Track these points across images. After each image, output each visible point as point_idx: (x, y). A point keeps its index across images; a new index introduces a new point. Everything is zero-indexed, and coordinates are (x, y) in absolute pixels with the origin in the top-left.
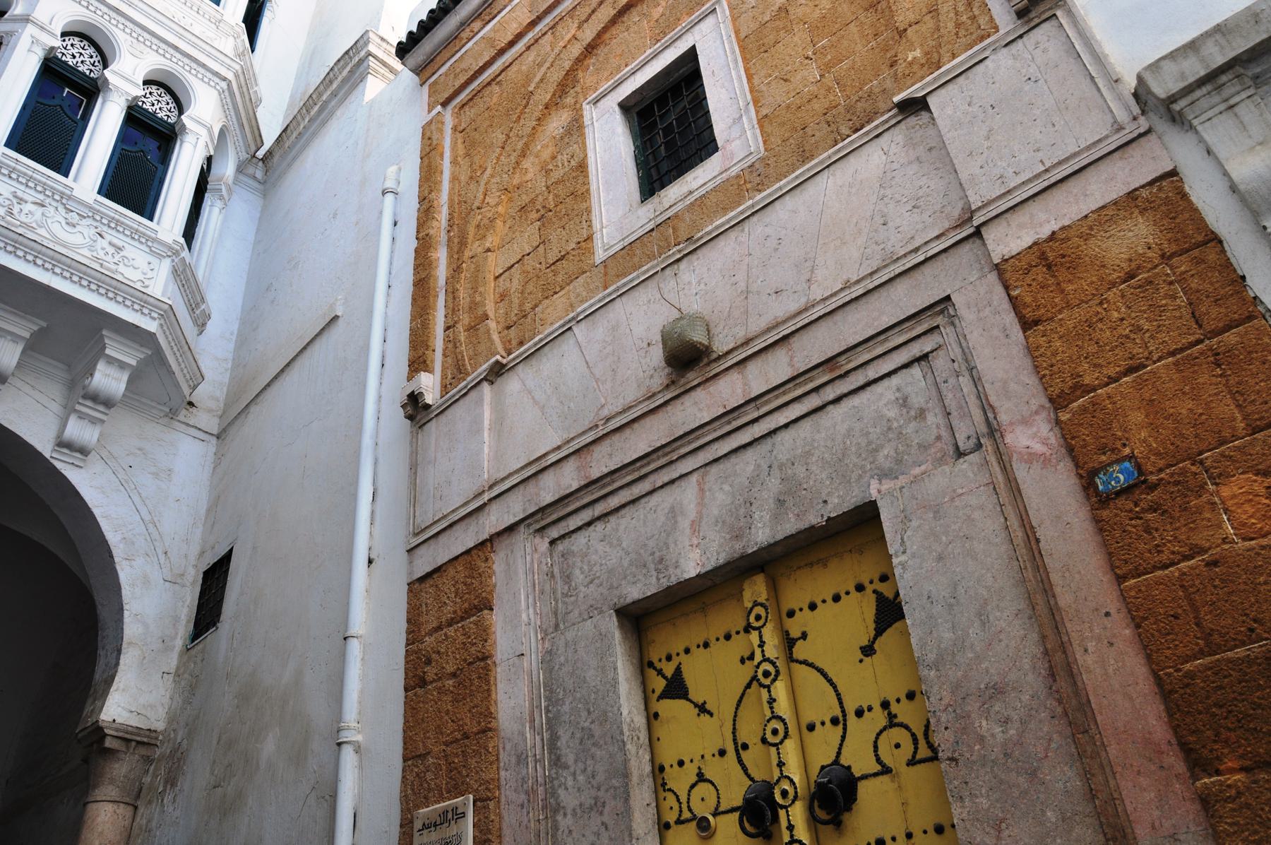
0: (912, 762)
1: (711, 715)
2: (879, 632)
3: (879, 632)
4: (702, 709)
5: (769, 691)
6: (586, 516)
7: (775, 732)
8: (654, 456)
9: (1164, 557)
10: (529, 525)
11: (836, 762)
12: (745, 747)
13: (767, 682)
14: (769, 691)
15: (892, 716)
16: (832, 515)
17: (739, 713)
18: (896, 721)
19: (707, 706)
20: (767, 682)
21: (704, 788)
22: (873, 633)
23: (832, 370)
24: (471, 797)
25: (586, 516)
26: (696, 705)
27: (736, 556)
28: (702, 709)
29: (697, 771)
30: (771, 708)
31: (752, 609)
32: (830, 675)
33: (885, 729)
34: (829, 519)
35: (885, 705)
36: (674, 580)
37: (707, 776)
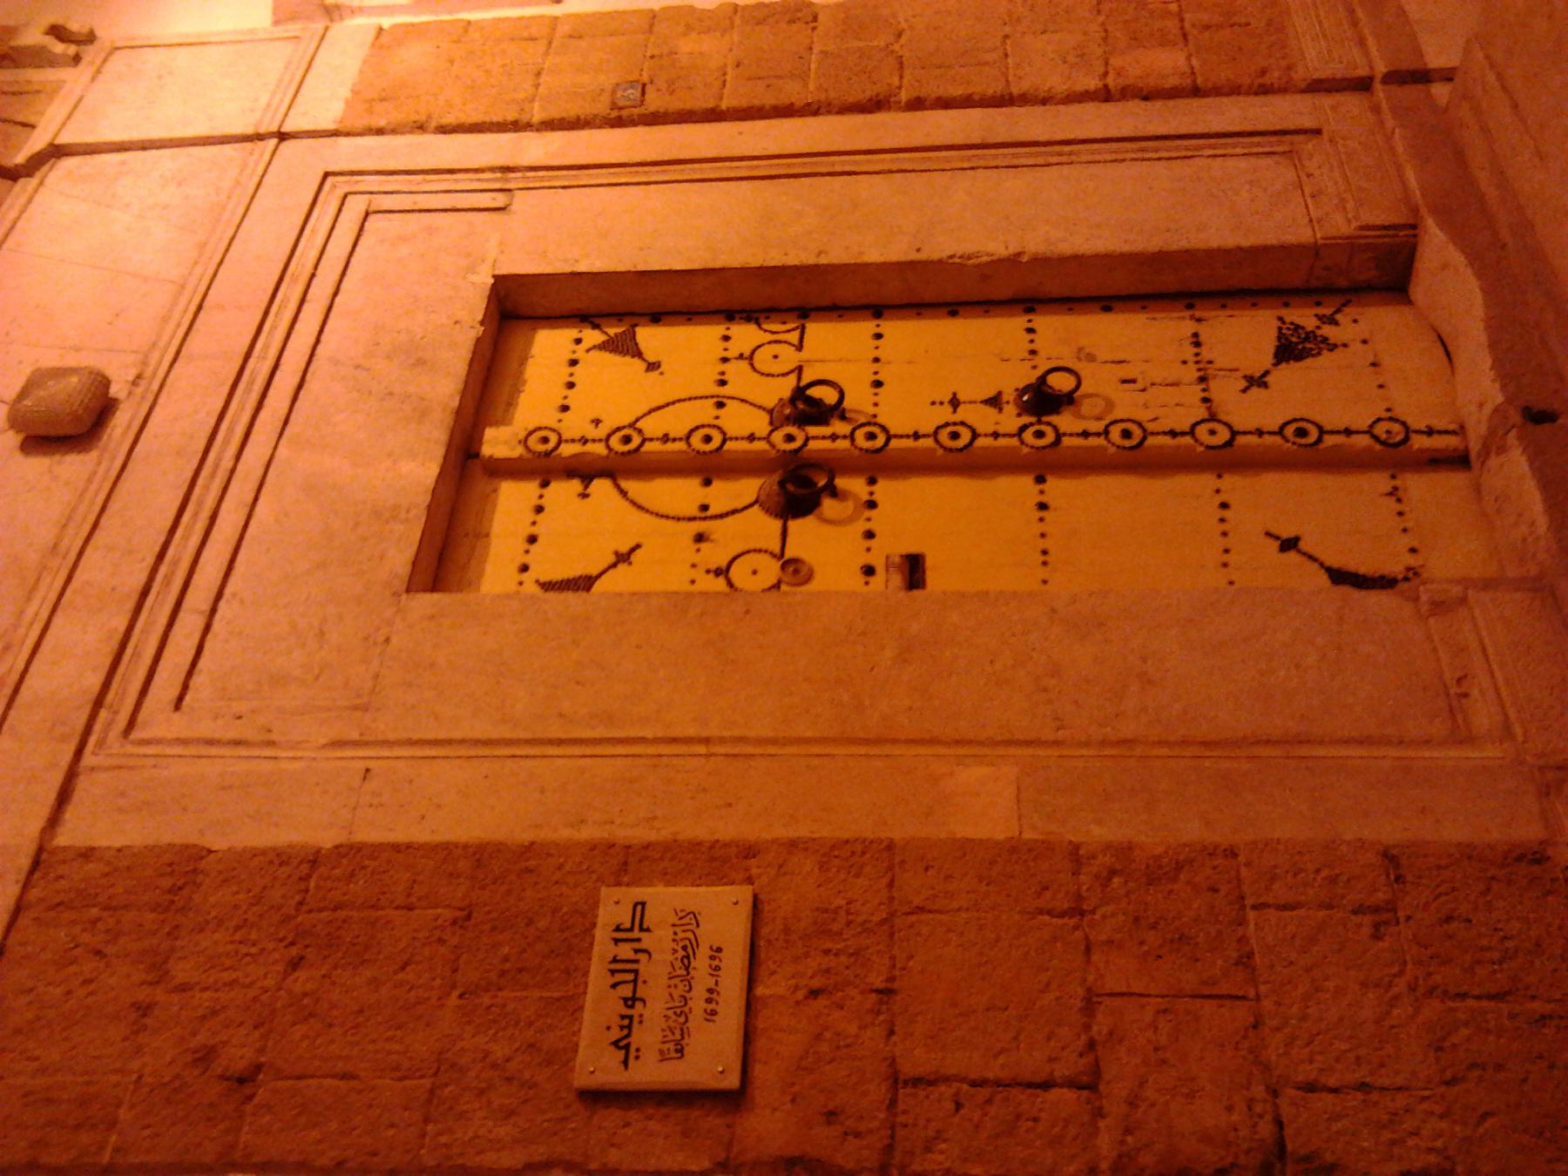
0: (800, 347)
1: (638, 546)
2: (638, 354)
3: (638, 354)
4: (623, 558)
5: (651, 440)
6: (189, 624)
7: (708, 439)
8: (197, 491)
9: (718, 84)
10: (101, 744)
11: (770, 412)
12: (705, 508)
13: (636, 441)
14: (651, 440)
15: (741, 356)
16: (480, 317)
17: (656, 509)
18: (747, 354)
19: (624, 549)
20: (636, 441)
21: (739, 573)
22: (636, 361)
23: (295, 280)
24: (604, 891)
25: (189, 624)
26: (614, 566)
27: (449, 420)
28: (623, 558)
29: (711, 576)
30: (674, 440)
31: (527, 447)
32: (662, 402)
33: (752, 365)
34: (482, 323)
35: (725, 360)
36: (425, 499)
37: (724, 564)
